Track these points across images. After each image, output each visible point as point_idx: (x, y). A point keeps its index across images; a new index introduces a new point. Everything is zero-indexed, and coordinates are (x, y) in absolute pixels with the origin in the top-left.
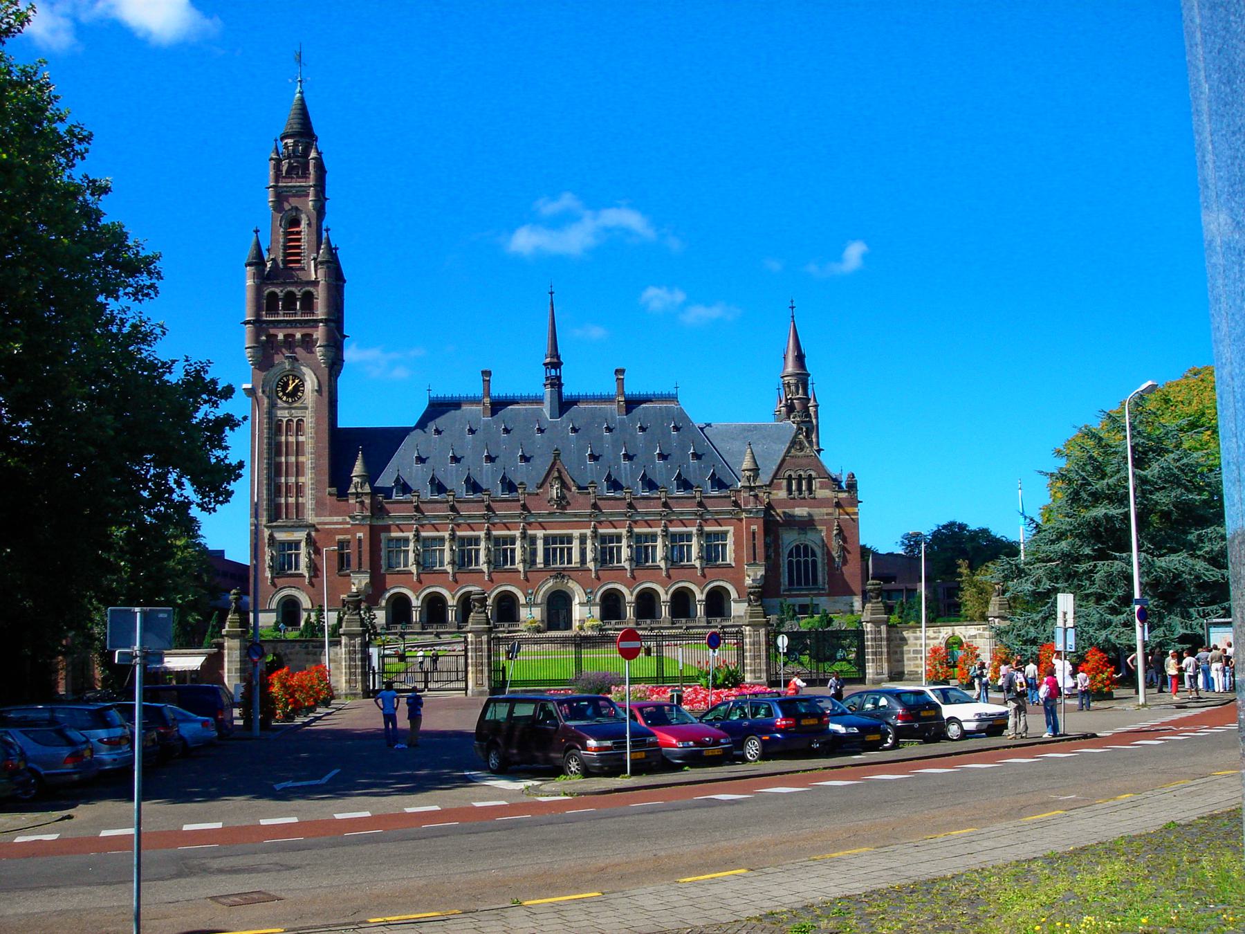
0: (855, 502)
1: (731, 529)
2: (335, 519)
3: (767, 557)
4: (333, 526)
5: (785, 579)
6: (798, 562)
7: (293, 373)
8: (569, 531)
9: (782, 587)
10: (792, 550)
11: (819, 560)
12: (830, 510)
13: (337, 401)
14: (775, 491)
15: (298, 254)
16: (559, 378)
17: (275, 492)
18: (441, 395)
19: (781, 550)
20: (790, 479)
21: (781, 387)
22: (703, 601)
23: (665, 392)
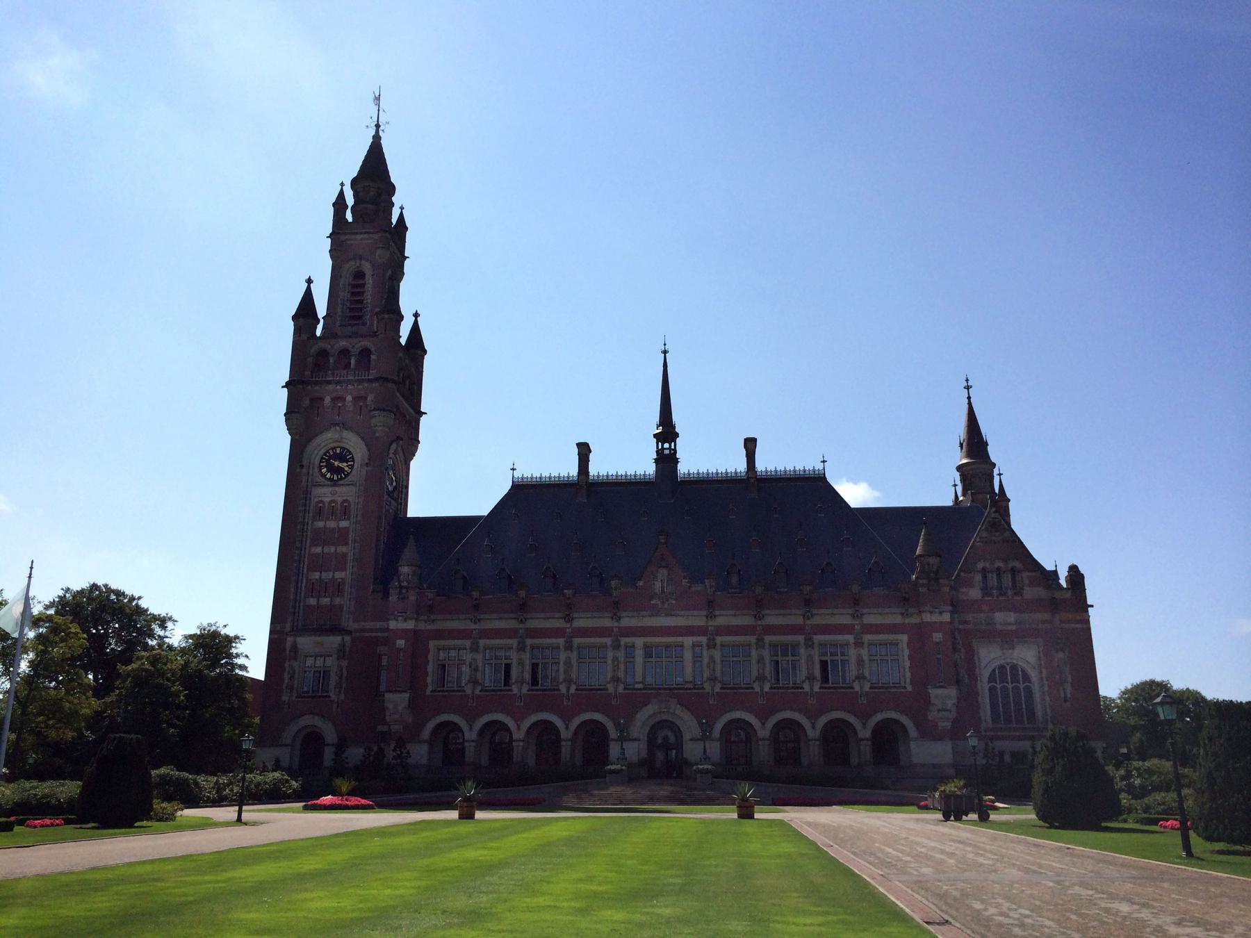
0: (1081, 605)
1: (904, 638)
2: (378, 625)
3: (958, 682)
4: (374, 634)
5: (986, 712)
6: (1004, 689)
7: (342, 445)
8: (680, 639)
9: (983, 725)
10: (994, 670)
11: (1036, 688)
12: (1046, 616)
13: (407, 487)
14: (964, 590)
15: (361, 309)
16: (675, 450)
17: (305, 594)
18: (527, 474)
19: (977, 670)
20: (984, 572)
21: (958, 482)
22: (867, 740)
23: (809, 467)
